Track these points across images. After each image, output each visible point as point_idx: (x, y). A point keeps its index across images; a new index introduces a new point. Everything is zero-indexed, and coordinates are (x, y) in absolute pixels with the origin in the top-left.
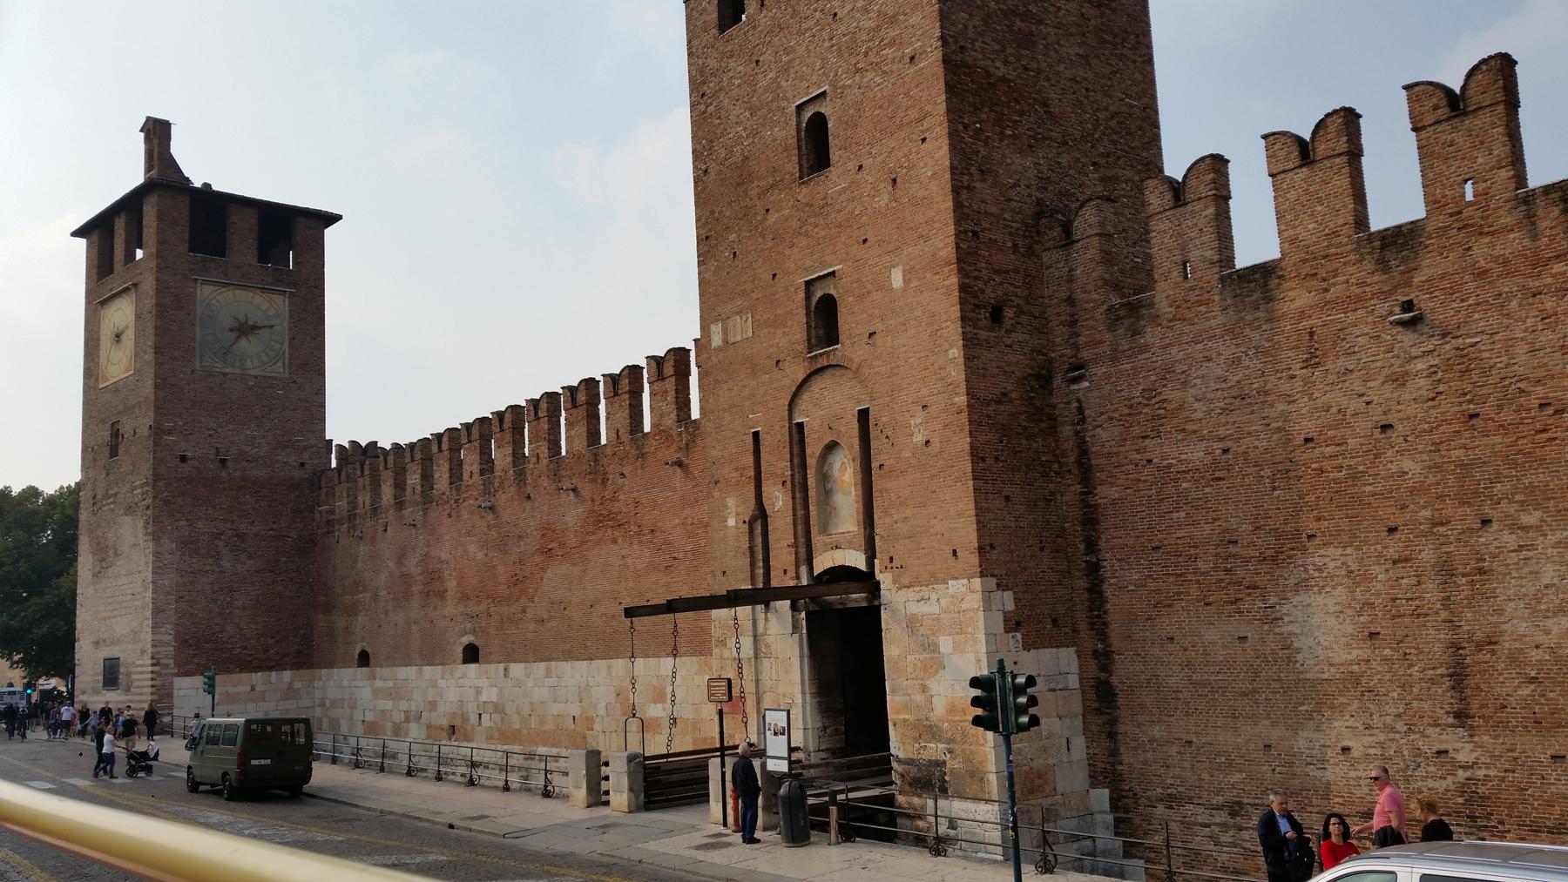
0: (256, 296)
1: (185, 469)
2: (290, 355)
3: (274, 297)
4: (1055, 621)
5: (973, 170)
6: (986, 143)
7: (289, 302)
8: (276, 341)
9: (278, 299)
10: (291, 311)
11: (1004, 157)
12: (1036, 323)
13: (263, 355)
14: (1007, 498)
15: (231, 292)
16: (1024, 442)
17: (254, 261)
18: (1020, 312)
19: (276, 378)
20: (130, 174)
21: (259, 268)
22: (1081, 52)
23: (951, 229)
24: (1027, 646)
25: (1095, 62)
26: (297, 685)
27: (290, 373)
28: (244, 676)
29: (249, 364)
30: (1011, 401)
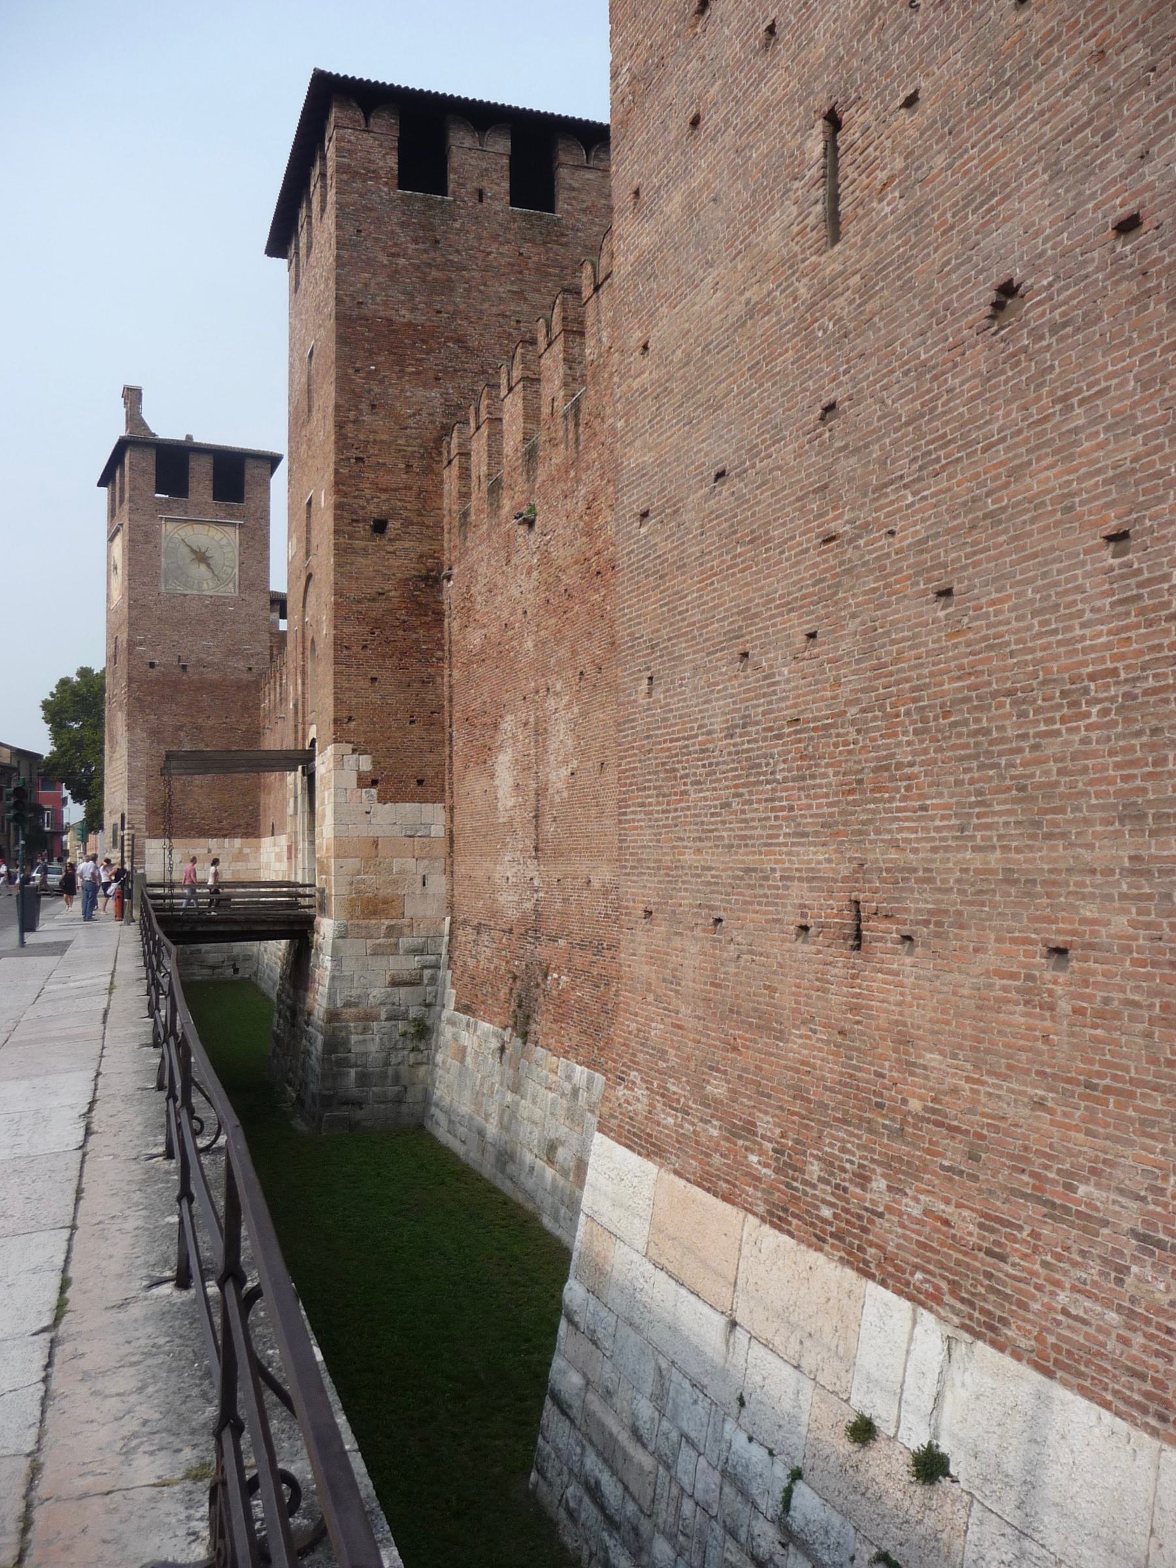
1: (153, 673)
4: (420, 782)
5: (364, 406)
6: (381, 382)
11: (402, 391)
12: (429, 532)
14: (374, 680)
16: (401, 633)
17: (210, 500)
18: (407, 523)
20: (119, 429)
22: (515, 288)
23: (332, 458)
24: (382, 800)
25: (531, 296)
26: (246, 851)
28: (202, 841)
29: (205, 586)
30: (388, 599)
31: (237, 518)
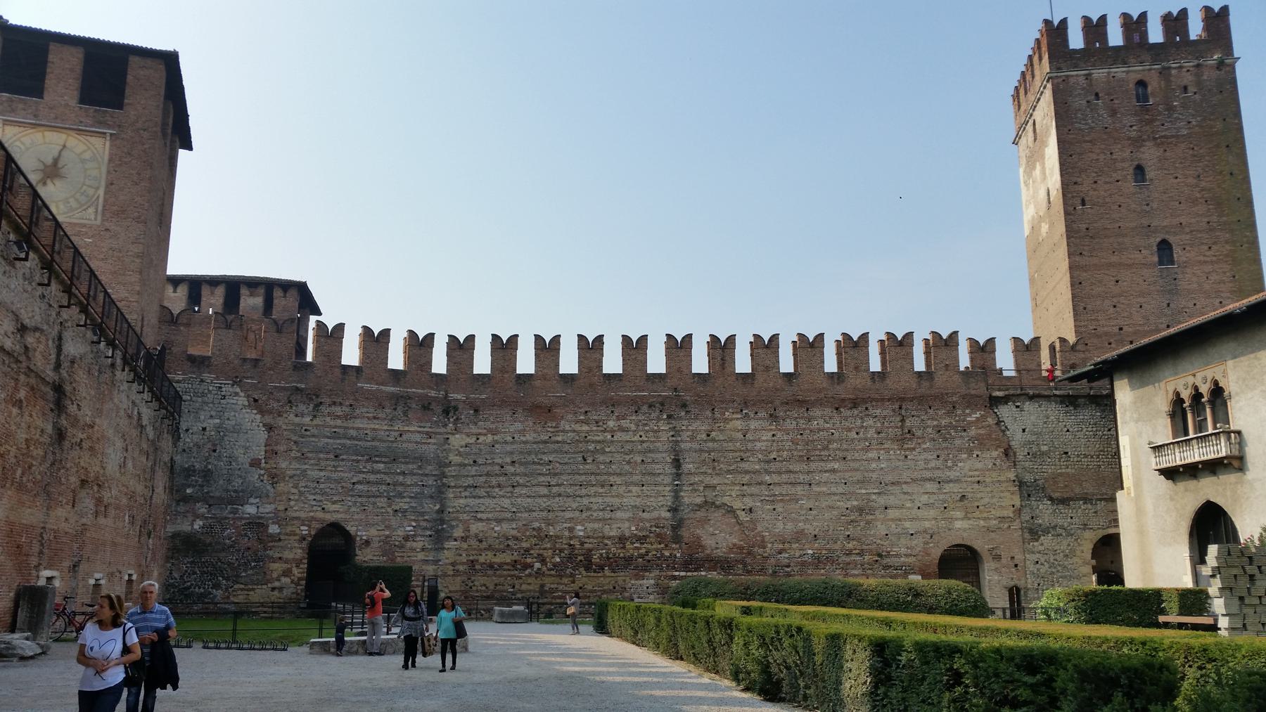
0: (70, 138)
2: (105, 200)
3: (93, 140)
7: (111, 146)
8: (89, 186)
9: (97, 142)
10: (111, 155)
13: (71, 200)
15: (41, 134)
17: (73, 102)
19: (84, 226)
21: (77, 109)
27: (103, 220)
31: (109, 127)
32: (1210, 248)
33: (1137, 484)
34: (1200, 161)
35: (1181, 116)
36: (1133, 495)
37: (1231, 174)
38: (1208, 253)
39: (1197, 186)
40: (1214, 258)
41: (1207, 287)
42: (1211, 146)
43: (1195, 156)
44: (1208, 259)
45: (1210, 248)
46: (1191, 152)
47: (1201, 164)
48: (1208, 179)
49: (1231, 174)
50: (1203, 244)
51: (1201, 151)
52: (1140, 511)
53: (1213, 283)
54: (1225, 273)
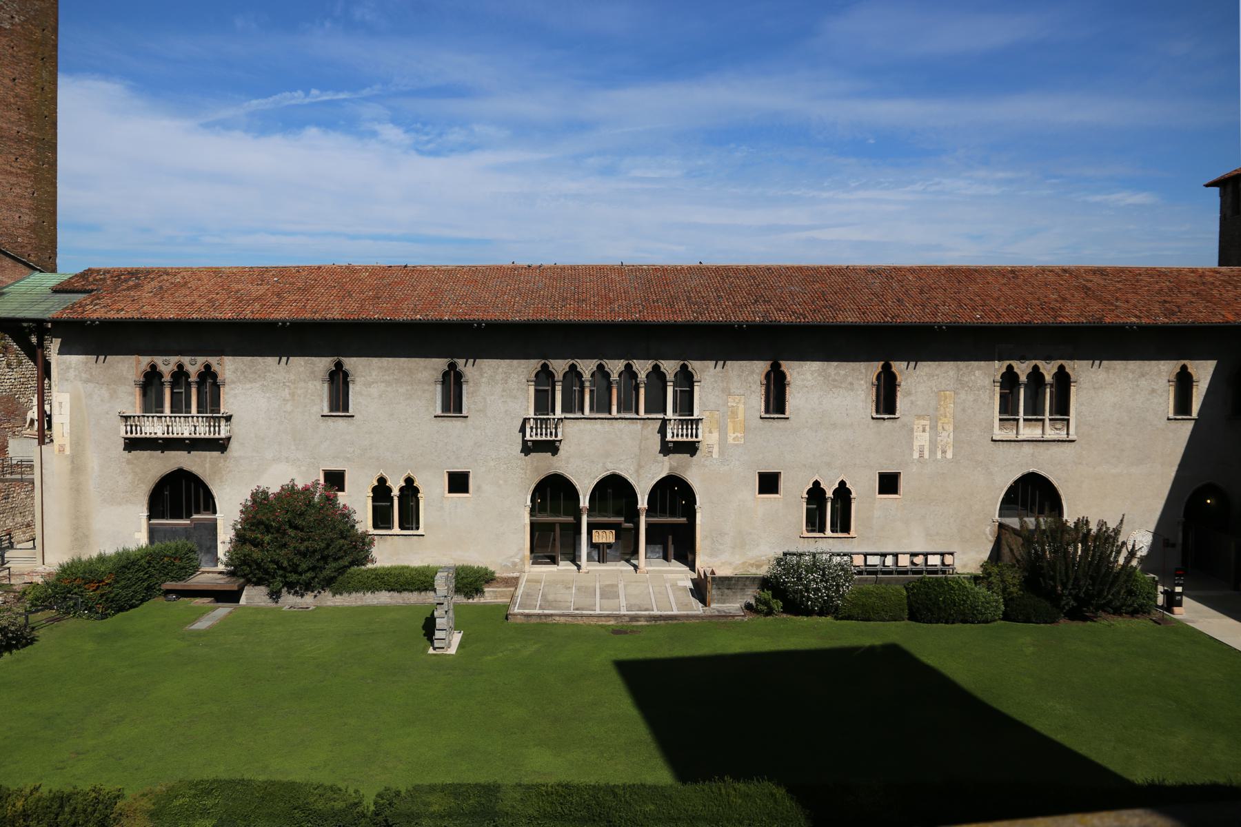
32: (17, 159)
33: (78, 442)
34: (17, 64)
35: (5, 7)
36: (68, 451)
37: (43, 89)
38: (14, 164)
39: (13, 90)
40: (19, 171)
41: (10, 199)
42: (29, 52)
43: (14, 57)
44: (14, 170)
45: (17, 159)
46: (11, 51)
47: (18, 68)
48: (23, 87)
49: (43, 89)
50: (11, 153)
51: (20, 54)
52: (76, 466)
53: (15, 196)
54: (27, 188)
